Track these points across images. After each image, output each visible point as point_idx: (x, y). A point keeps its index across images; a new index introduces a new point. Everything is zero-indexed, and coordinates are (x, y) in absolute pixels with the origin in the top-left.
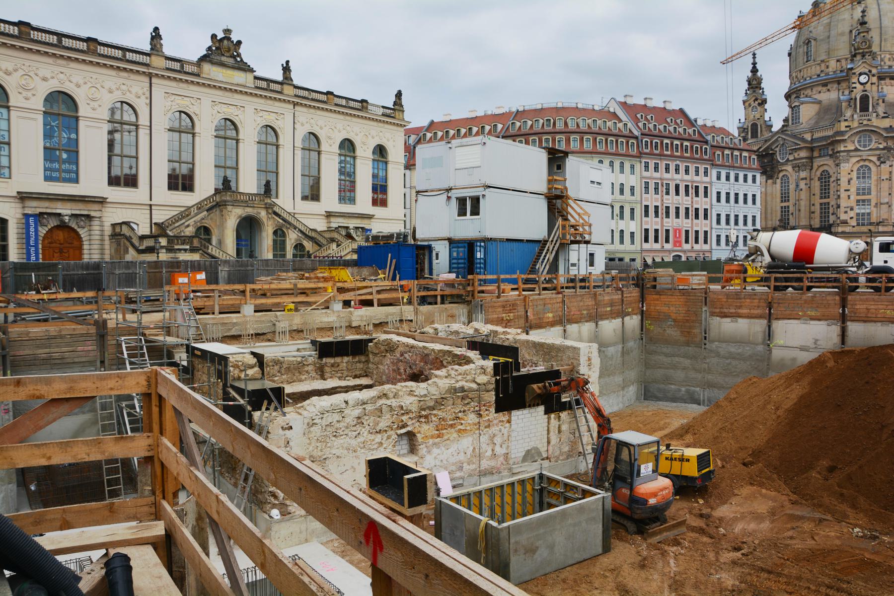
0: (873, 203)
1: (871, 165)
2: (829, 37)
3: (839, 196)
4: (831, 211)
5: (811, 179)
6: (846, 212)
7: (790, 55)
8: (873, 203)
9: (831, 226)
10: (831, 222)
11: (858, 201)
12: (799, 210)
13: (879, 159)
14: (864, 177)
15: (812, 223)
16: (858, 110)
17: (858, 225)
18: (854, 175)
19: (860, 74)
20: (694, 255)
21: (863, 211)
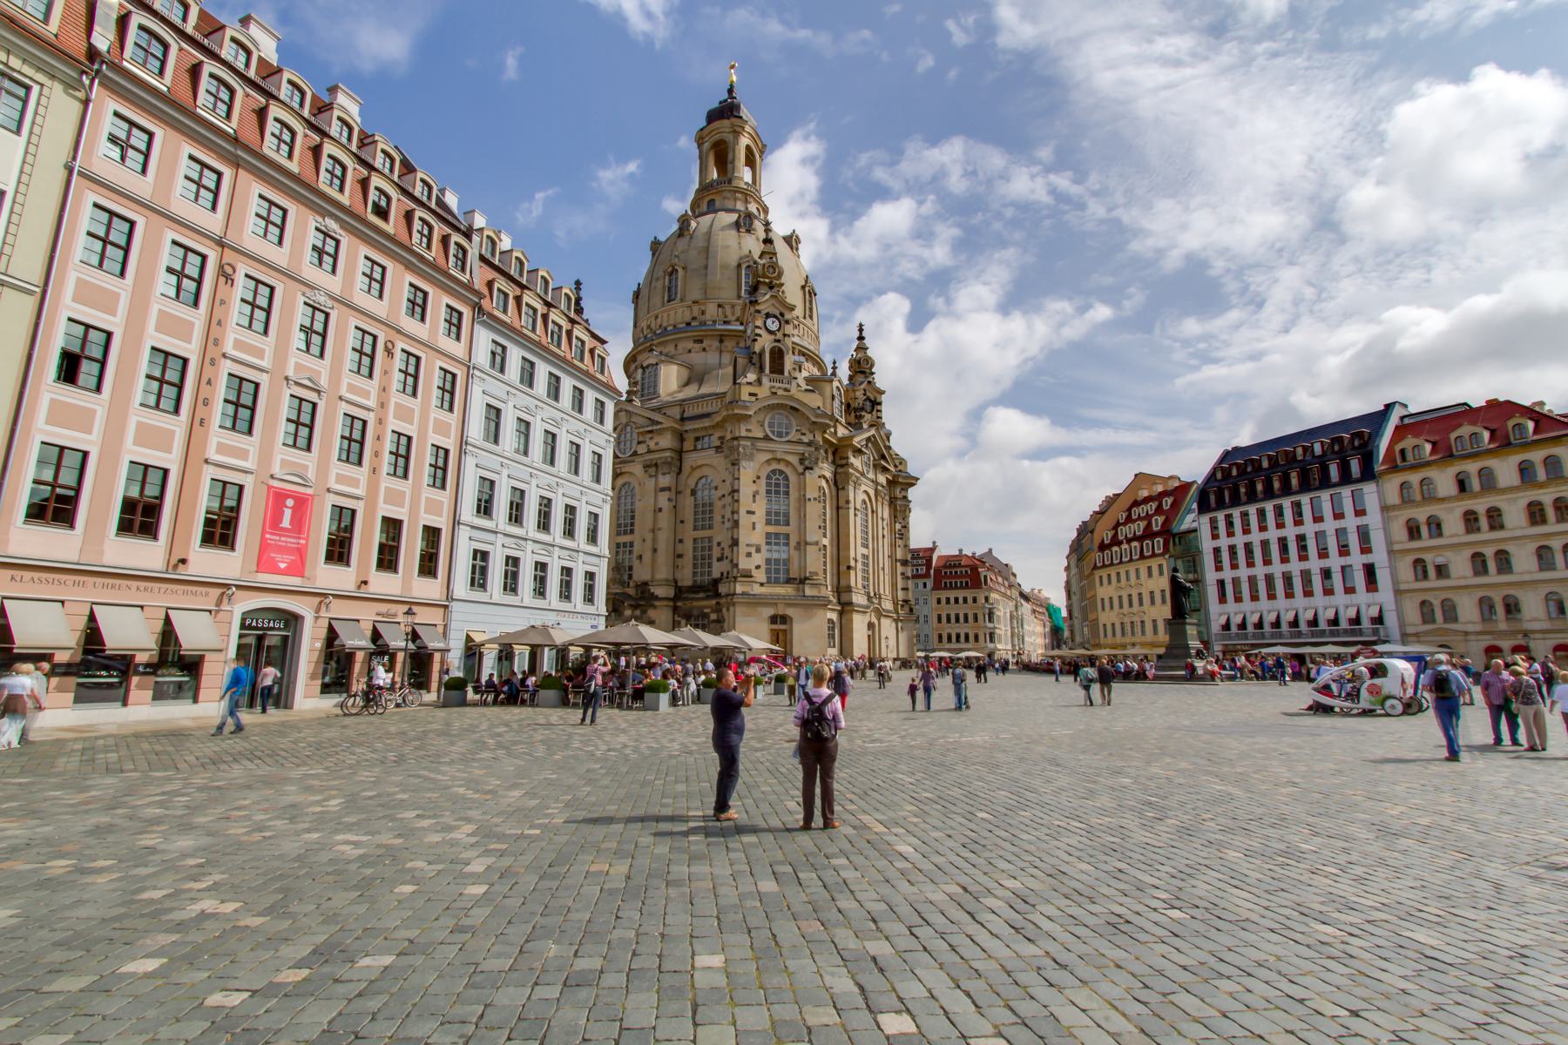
0: (793, 541)
1: (788, 471)
2: (706, 267)
3: (736, 524)
4: (716, 553)
5: (678, 493)
6: (749, 555)
7: (637, 295)
8: (793, 541)
9: (716, 582)
10: (716, 575)
11: (768, 535)
12: (655, 550)
13: (802, 461)
14: (777, 492)
15: (679, 576)
16: (767, 370)
17: (769, 582)
18: (762, 486)
19: (768, 316)
20: (367, 615)
21: (775, 556)
